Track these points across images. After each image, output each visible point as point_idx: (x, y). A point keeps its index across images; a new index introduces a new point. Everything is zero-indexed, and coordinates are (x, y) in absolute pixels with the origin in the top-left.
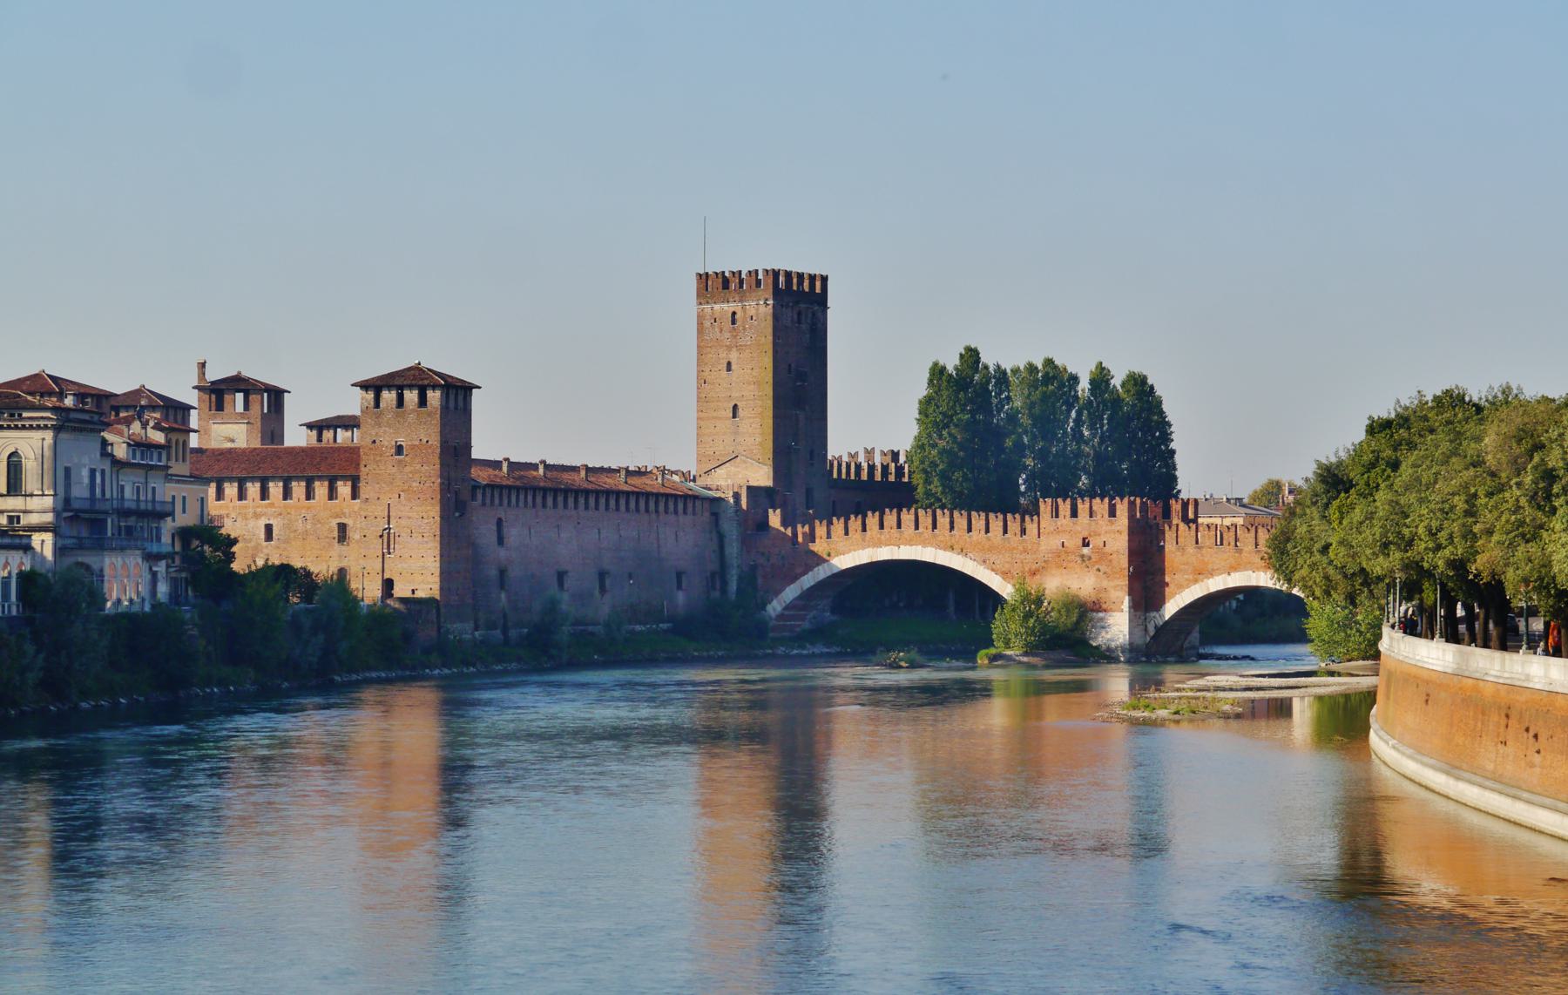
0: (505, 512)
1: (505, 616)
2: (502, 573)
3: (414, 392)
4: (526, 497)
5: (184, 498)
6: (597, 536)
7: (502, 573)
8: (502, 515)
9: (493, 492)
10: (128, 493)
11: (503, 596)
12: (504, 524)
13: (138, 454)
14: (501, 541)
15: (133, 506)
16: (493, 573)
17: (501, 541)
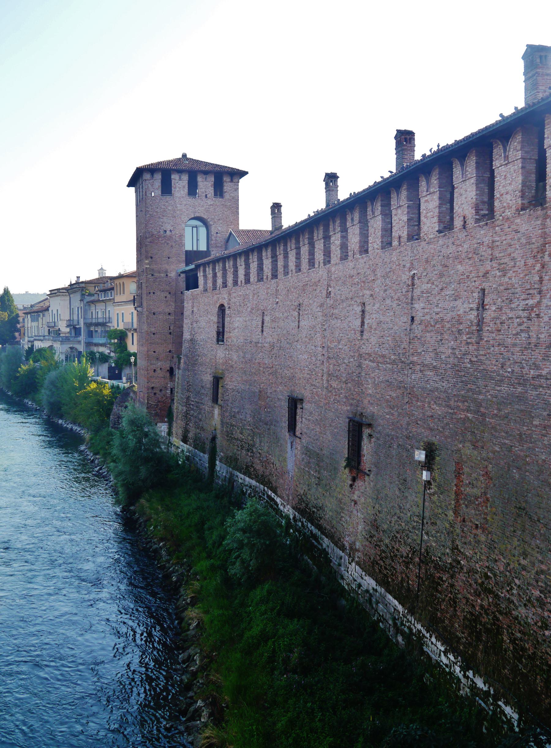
0: (230, 294)
1: (214, 439)
2: (217, 380)
3: (208, 179)
4: (298, 255)
5: (123, 314)
6: (358, 322)
7: (217, 380)
8: (223, 297)
9: (214, 269)
10: (100, 315)
11: (216, 411)
12: (227, 312)
13: (103, 295)
14: (220, 335)
15: (100, 321)
16: (208, 379)
17: (220, 335)
